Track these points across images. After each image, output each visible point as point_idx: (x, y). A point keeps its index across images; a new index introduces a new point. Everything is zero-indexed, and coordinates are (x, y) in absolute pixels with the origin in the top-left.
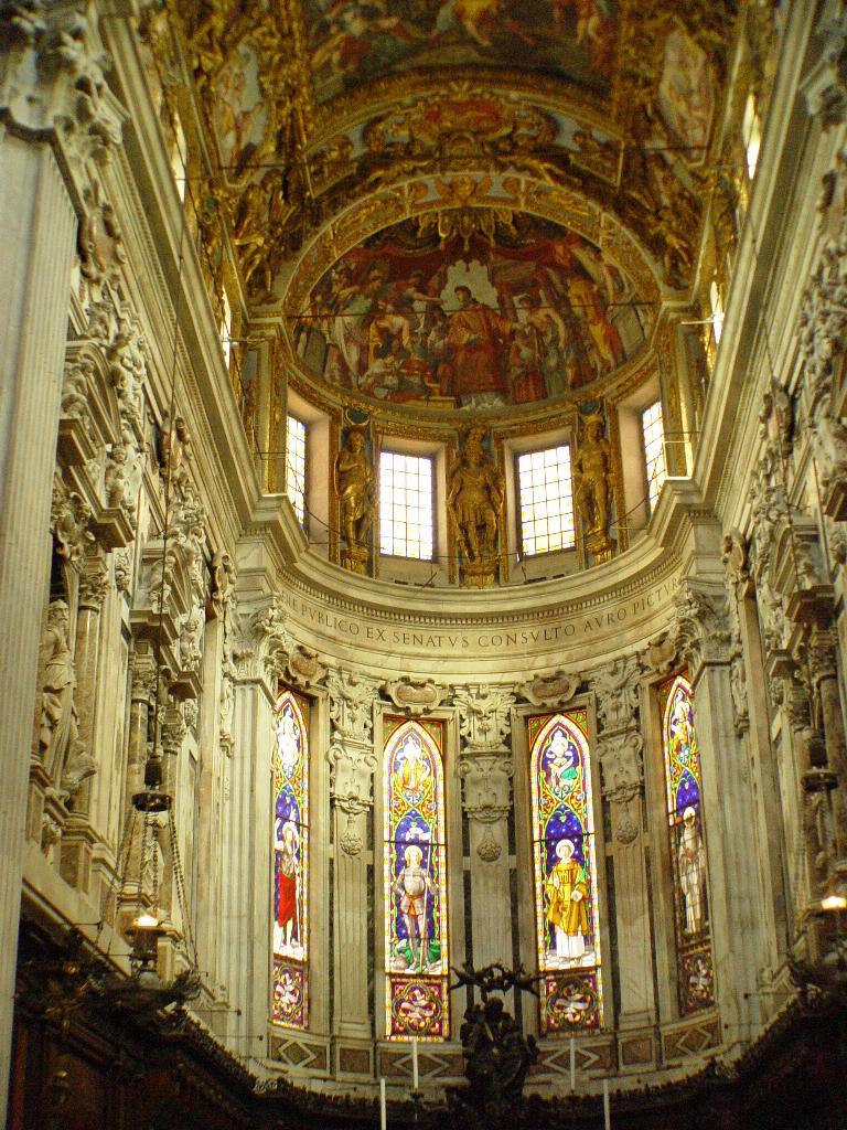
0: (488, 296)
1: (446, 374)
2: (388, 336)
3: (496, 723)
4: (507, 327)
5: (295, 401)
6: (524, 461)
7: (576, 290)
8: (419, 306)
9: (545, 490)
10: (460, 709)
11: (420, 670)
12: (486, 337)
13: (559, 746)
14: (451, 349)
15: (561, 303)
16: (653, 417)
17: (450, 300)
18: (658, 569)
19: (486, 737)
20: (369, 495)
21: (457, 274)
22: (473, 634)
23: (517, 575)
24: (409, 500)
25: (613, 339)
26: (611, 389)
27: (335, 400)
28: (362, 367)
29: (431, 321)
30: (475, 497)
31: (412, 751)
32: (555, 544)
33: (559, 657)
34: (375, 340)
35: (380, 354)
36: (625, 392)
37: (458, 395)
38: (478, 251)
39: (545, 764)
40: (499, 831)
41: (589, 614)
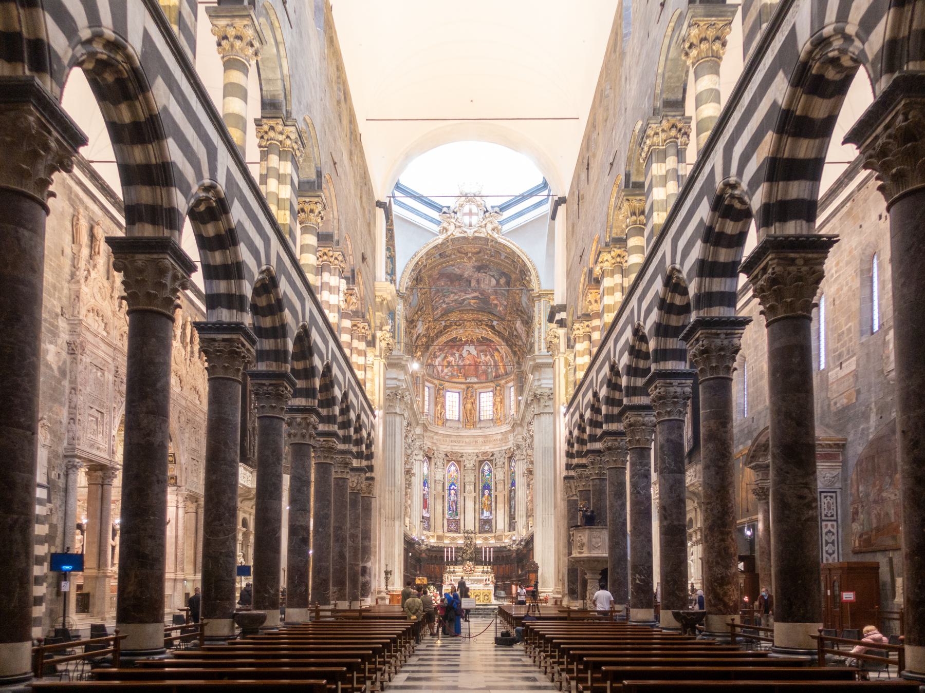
0: (474, 353)
1: (463, 371)
2: (449, 363)
3: (472, 462)
4: (478, 360)
5: (427, 384)
6: (482, 395)
7: (496, 354)
8: (457, 355)
9: (486, 401)
10: (464, 458)
11: (456, 449)
12: (473, 363)
13: (486, 468)
14: (464, 365)
15: (492, 356)
16: (512, 389)
17: (465, 354)
18: (510, 431)
19: (469, 465)
20: (443, 406)
21: (466, 348)
22: (467, 440)
23: (478, 426)
24: (453, 402)
25: (505, 369)
26: (503, 382)
27: (436, 382)
28: (442, 371)
29: (460, 358)
30: (469, 406)
31: (453, 468)
32: (488, 417)
33: (487, 447)
34: (445, 363)
35: (447, 367)
36: (506, 383)
37: (466, 377)
38: (472, 342)
39: (483, 472)
40: (472, 487)
41: (495, 437)
